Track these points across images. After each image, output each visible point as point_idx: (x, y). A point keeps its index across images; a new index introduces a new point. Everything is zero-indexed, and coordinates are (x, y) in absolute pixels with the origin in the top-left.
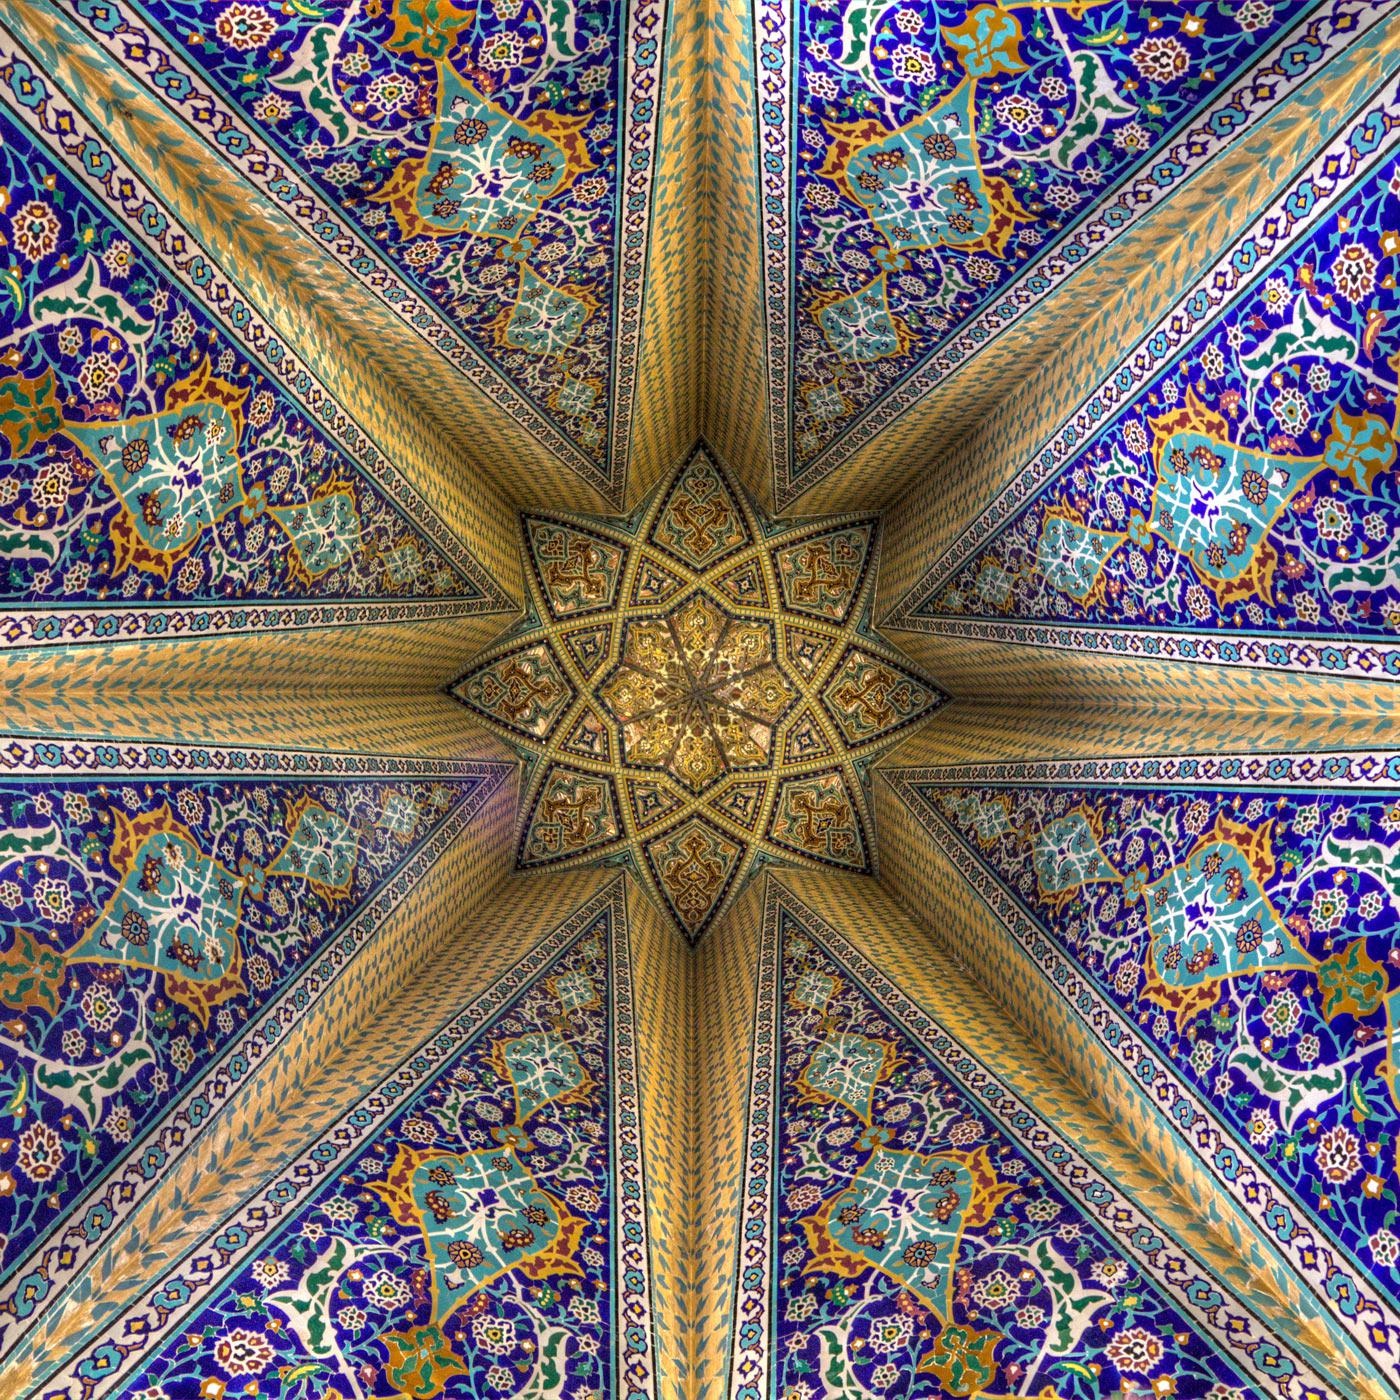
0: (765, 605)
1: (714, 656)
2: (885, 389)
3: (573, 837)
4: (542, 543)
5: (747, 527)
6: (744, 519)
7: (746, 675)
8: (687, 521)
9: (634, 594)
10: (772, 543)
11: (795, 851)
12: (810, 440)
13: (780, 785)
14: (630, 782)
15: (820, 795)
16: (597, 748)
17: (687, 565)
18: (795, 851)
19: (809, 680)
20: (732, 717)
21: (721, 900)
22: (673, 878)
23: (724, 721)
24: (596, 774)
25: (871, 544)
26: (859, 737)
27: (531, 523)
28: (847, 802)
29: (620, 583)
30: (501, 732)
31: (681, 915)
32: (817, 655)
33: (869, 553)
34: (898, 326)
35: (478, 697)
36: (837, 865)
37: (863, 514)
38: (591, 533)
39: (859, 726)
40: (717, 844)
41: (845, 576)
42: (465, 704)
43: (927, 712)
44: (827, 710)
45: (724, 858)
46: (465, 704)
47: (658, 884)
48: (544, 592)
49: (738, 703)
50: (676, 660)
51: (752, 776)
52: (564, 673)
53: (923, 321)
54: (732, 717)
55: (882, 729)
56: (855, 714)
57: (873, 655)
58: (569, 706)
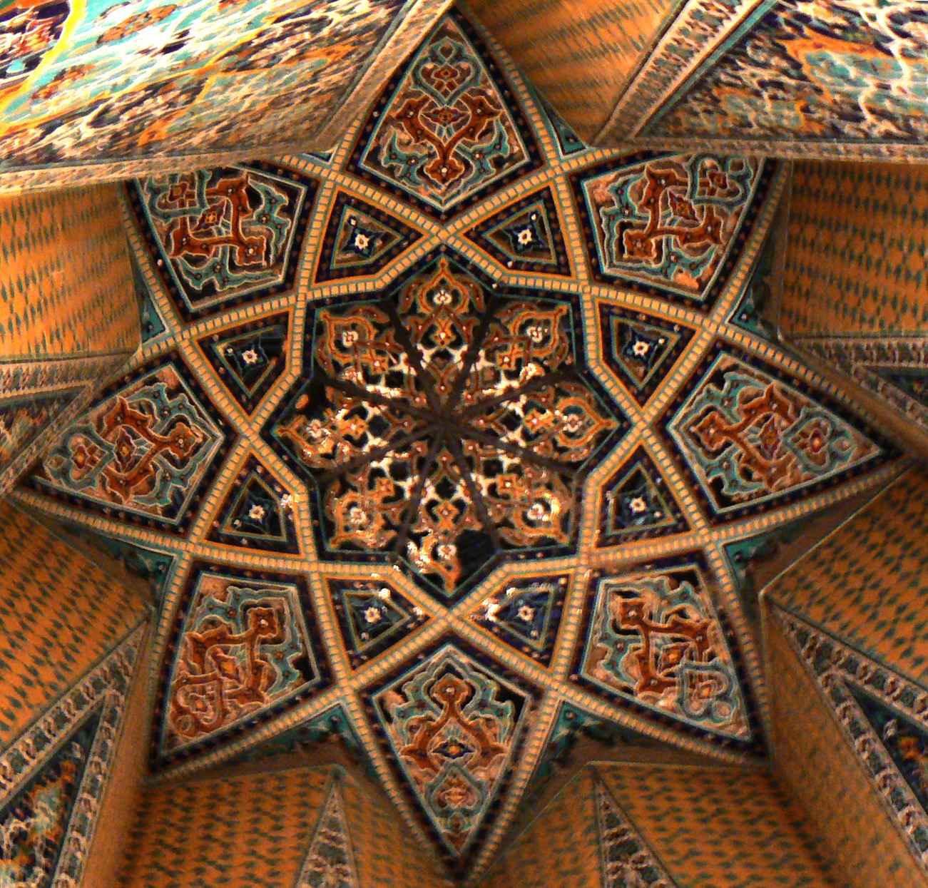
0: (642, 397)
1: (511, 395)
3: (115, 482)
4: (434, 58)
5: (720, 286)
6: (726, 273)
7: (529, 457)
9: (486, 225)
10: (733, 334)
11: (386, 748)
14: (252, 463)
17: (592, 253)
18: (386, 748)
21: (237, 733)
22: (200, 647)
23: (445, 490)
24: (217, 415)
25: (857, 472)
26: (599, 675)
28: (507, 747)
29: (483, 195)
30: (142, 259)
33: (842, 478)
36: (425, 822)
38: (512, 101)
39: (612, 665)
40: (293, 647)
41: (782, 470)
43: (718, 740)
44: (589, 602)
52: (297, 247)
55: (638, 699)
58: (264, 295)
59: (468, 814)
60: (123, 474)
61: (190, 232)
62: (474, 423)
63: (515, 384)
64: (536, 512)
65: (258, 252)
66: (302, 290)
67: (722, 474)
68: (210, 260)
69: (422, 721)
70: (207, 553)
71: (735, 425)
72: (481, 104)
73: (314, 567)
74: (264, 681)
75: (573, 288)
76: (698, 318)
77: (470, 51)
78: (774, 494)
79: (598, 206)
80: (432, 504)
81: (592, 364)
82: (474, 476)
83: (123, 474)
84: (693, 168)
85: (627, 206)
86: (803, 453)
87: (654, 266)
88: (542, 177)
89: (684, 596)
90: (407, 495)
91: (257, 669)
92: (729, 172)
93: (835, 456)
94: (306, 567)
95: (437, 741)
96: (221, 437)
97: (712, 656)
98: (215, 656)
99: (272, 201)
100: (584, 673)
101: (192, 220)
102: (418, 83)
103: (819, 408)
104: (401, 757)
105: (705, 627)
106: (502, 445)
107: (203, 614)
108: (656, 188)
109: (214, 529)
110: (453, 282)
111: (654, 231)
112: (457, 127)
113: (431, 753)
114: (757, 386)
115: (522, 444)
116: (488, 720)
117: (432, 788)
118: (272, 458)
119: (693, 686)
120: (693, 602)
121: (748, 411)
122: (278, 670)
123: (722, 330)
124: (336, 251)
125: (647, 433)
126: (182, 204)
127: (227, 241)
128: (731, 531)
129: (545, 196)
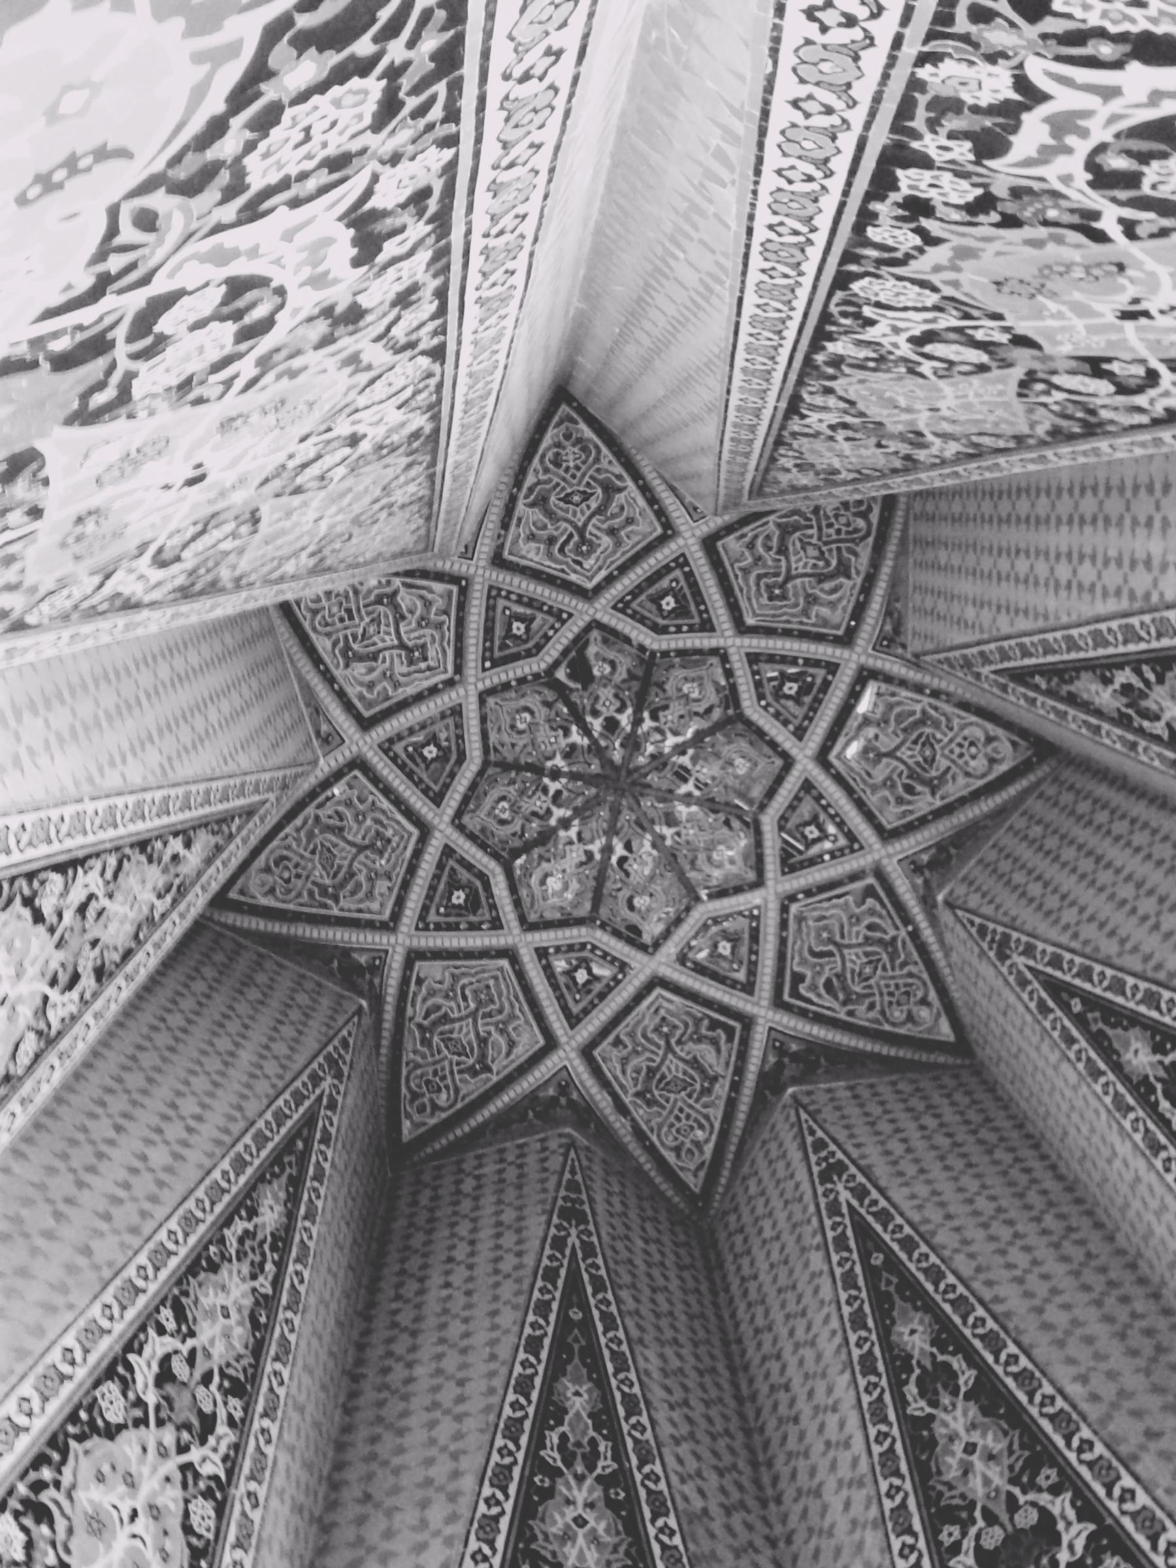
0: (448, 851)
1: (565, 823)
2: (129, 1347)
3: (936, 724)
4: (697, 1144)
5: (405, 981)
8: (483, 1041)
12: (270, 1216)
13: (598, 590)
14: (800, 733)
15: (551, 541)
16: (806, 809)
18: (646, 490)
19: (457, 712)
20: (597, 725)
22: (844, 570)
23: (611, 725)
24: (839, 779)
26: (438, 587)
27: (695, 1183)
28: (521, 508)
29: (626, 1010)
30: (928, 934)
31: (874, 517)
32: (419, 738)
34: (70, 1531)
35: (924, 1002)
37: (230, 918)
40: (746, 571)
41: (311, 836)
42: (949, 1008)
44: (459, 653)
45: (751, 546)
46: (949, 1008)
47: (870, 581)
48: (740, 1071)
49: (576, 737)
50: (619, 850)
51: (624, 625)
53: (29, 1546)
54: (597, 725)
56: (423, 622)
57: (341, 695)
58: (808, 893)
59: (558, 445)
60: (928, 730)
61: (885, 957)
62: (594, 791)
63: (562, 833)
64: (524, 721)
65: (819, 935)
66: (772, 897)
67: (361, 807)
68: (861, 928)
69: (614, 516)
70: (838, 652)
71: (361, 857)
72: (650, 1103)
73: (730, 642)
74: (775, 539)
75: (529, 937)
76: (415, 943)
77: (670, 1157)
78: (310, 810)
79: (527, 1022)
80: (620, 710)
81: (498, 870)
82: (586, 741)
83: (928, 730)
84: (457, 1090)
85: (502, 1032)
86: (296, 859)
87: (465, 981)
88: (579, 1039)
89: (371, 686)
90: (646, 714)
91: (783, 550)
92: (426, 1100)
93: (267, 870)
94: (738, 641)
95: (594, 505)
96: (832, 757)
97: (335, 644)
98: (828, 564)
99: (813, 988)
100: (455, 589)
101: (884, 968)
102: (707, 1117)
103: (291, 907)
104: (630, 483)
105: (347, 666)
106: (565, 775)
107: (840, 599)
108: (483, 1056)
109: (834, 673)
110: (634, 918)
111: (474, 1015)
112: (663, 1077)
113: (599, 491)
114: (347, 905)
115: (546, 780)
116: (544, 527)
117: (597, 460)
118: (779, 739)
119: (349, 611)
120: (361, 684)
121: (351, 874)
122: (760, 550)
123: (392, 940)
124: (746, 936)
125: (436, 821)
126: (897, 986)
127: (849, 946)
128: (341, 759)
129: (573, 1021)
